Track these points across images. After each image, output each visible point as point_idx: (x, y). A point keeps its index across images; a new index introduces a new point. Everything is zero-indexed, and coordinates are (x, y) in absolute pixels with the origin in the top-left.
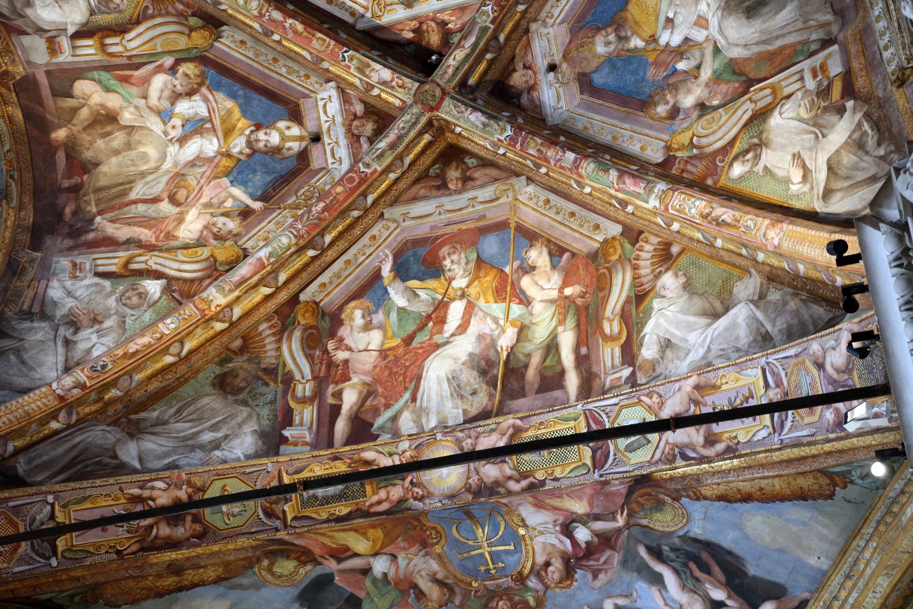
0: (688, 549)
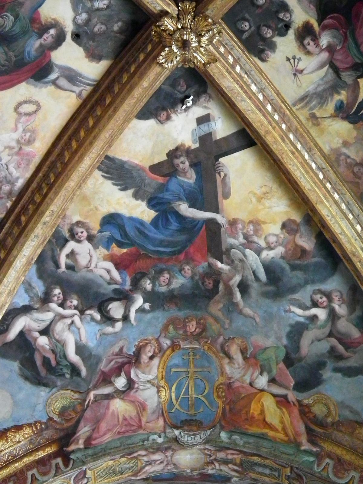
0: (53, 377)
